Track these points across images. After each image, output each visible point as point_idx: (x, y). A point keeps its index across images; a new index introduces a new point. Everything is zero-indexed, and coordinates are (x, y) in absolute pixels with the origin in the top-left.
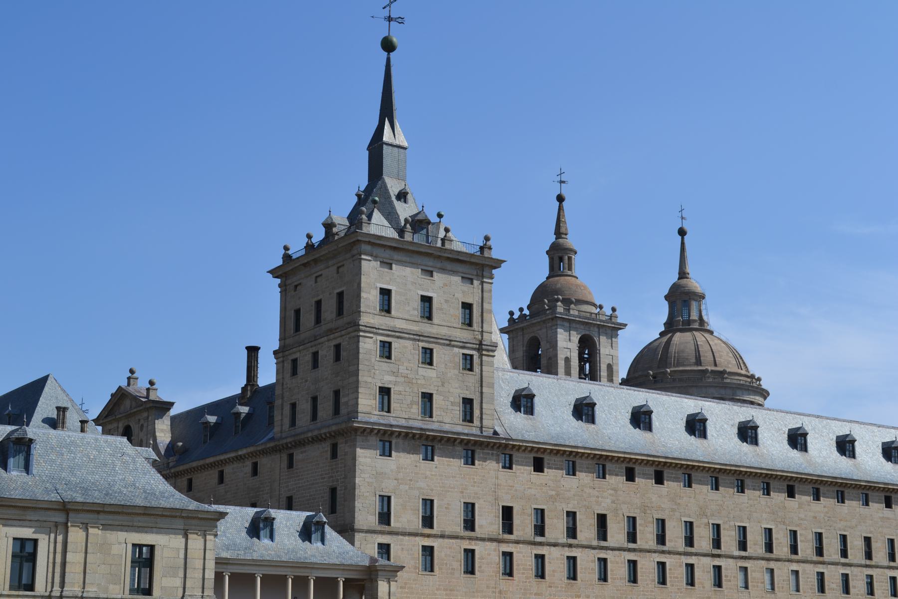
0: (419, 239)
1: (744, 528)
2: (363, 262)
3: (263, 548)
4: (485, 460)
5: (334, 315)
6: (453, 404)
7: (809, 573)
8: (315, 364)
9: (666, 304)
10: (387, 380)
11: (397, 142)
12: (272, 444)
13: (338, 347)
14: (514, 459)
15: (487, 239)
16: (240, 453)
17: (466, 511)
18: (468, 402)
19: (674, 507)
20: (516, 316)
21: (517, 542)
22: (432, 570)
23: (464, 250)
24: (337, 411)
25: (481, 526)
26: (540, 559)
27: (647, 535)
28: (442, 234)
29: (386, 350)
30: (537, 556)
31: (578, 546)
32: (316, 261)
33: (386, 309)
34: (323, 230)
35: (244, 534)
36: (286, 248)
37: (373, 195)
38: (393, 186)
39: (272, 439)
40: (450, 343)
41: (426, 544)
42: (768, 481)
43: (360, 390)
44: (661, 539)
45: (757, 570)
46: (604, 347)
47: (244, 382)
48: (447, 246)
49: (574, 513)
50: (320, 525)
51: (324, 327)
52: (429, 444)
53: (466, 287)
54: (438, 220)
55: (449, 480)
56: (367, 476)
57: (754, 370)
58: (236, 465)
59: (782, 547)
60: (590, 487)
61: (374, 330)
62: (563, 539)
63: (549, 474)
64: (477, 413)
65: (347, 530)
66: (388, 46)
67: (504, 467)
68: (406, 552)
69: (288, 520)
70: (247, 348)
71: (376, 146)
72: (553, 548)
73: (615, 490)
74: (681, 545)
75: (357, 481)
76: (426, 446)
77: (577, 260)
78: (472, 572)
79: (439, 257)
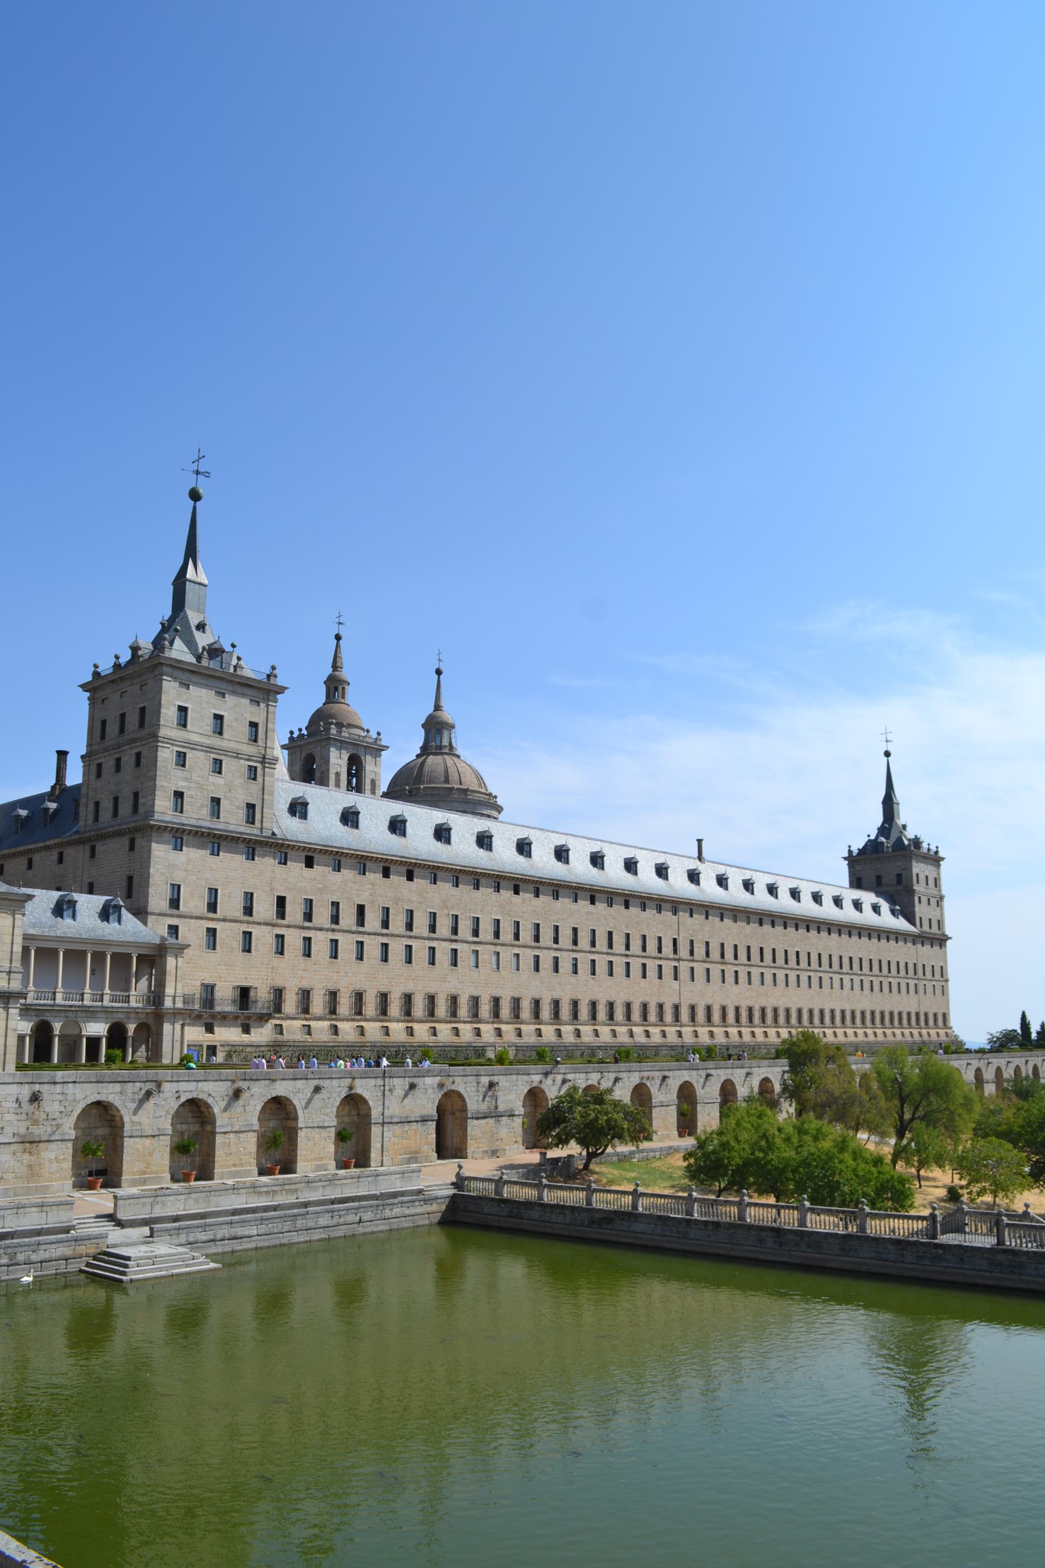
0: (214, 664)
1: (478, 919)
2: (164, 682)
3: (66, 926)
4: (263, 856)
5: (136, 727)
6: (238, 808)
7: (527, 956)
8: (118, 768)
9: (422, 732)
10: (181, 785)
11: (199, 580)
12: (77, 837)
13: (138, 755)
14: (289, 856)
15: (273, 668)
16: (48, 843)
17: (245, 899)
18: (251, 807)
20: (295, 735)
21: (289, 926)
22: (214, 949)
23: (253, 676)
25: (258, 913)
26: (308, 940)
27: (398, 923)
28: (234, 662)
29: (181, 759)
30: (305, 938)
31: (339, 931)
32: (122, 679)
33: (183, 724)
34: (130, 652)
35: (49, 914)
36: (96, 666)
37: (176, 624)
38: (194, 618)
39: (77, 832)
40: (237, 756)
41: (210, 926)
42: (498, 880)
43: (157, 793)
44: (409, 926)
45: (486, 953)
46: (369, 765)
47: (53, 781)
48: (239, 672)
49: (338, 903)
50: (118, 908)
51: (127, 737)
52: (216, 841)
53: (254, 708)
54: (231, 649)
55: (231, 872)
57: (492, 789)
58: (43, 854)
59: (507, 935)
61: (171, 741)
62: (328, 924)
63: (318, 869)
64: (258, 816)
65: (141, 913)
66: (195, 495)
67: (280, 863)
68: (192, 932)
69: (89, 903)
70: (57, 752)
71: (180, 582)
73: (372, 884)
74: (425, 931)
75: (152, 870)
76: (214, 843)
77: (349, 690)
78: (249, 951)
79: (231, 681)
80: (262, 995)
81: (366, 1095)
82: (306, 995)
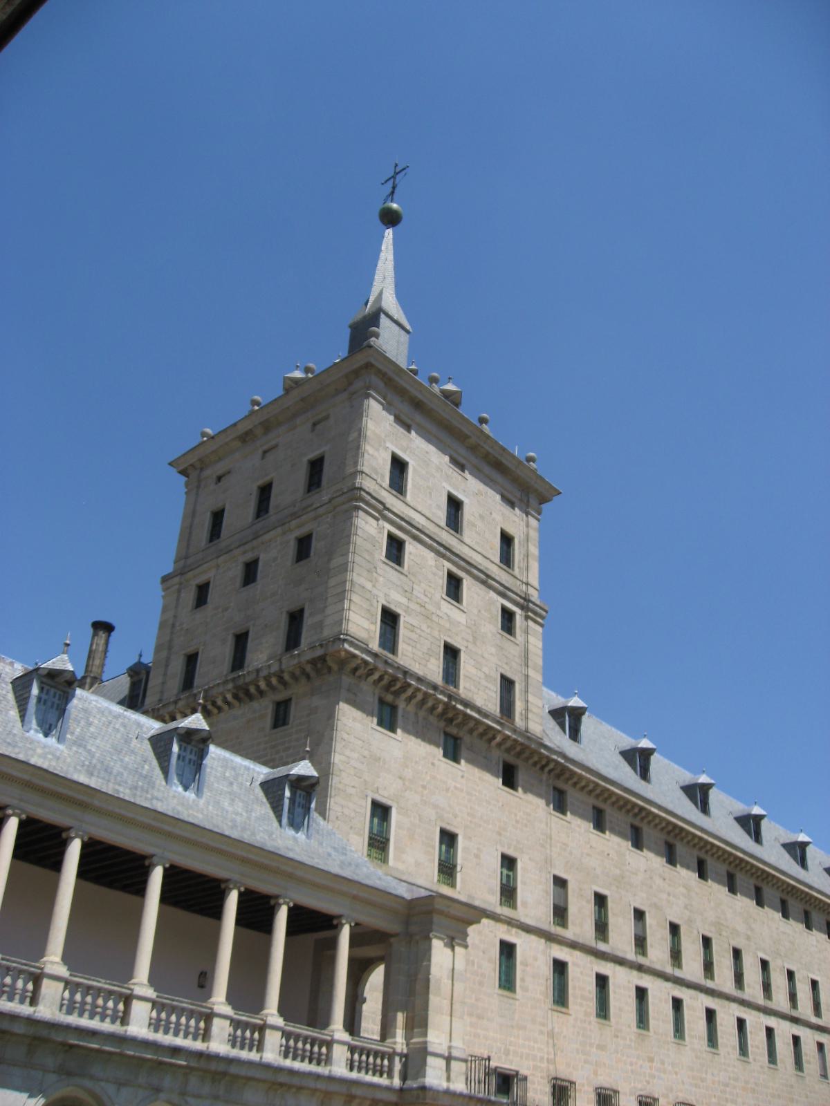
6: (487, 677)
10: (397, 601)
19: (749, 933)
29: (395, 549)
40: (485, 580)
52: (455, 731)
56: (355, 755)
60: (660, 876)
62: (630, 953)
64: (519, 706)
72: (618, 968)
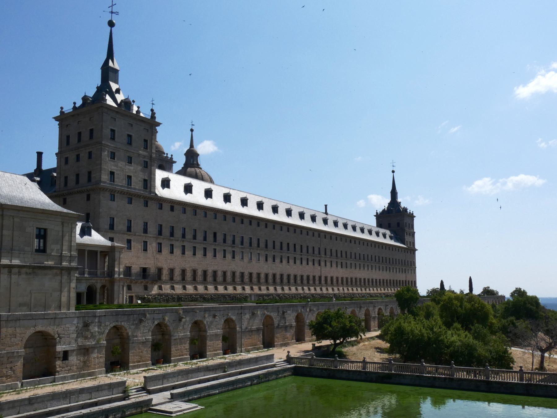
6: (139, 181)
10: (113, 168)
12: (56, 194)
13: (90, 154)
17: (144, 225)
18: (145, 181)
21: (163, 239)
24: (89, 180)
28: (137, 109)
32: (78, 115)
33: (113, 138)
36: (62, 108)
38: (114, 86)
39: (55, 191)
43: (102, 172)
64: (149, 185)
66: (111, 24)
80: (153, 271)
81: (234, 318)
82: (172, 271)
